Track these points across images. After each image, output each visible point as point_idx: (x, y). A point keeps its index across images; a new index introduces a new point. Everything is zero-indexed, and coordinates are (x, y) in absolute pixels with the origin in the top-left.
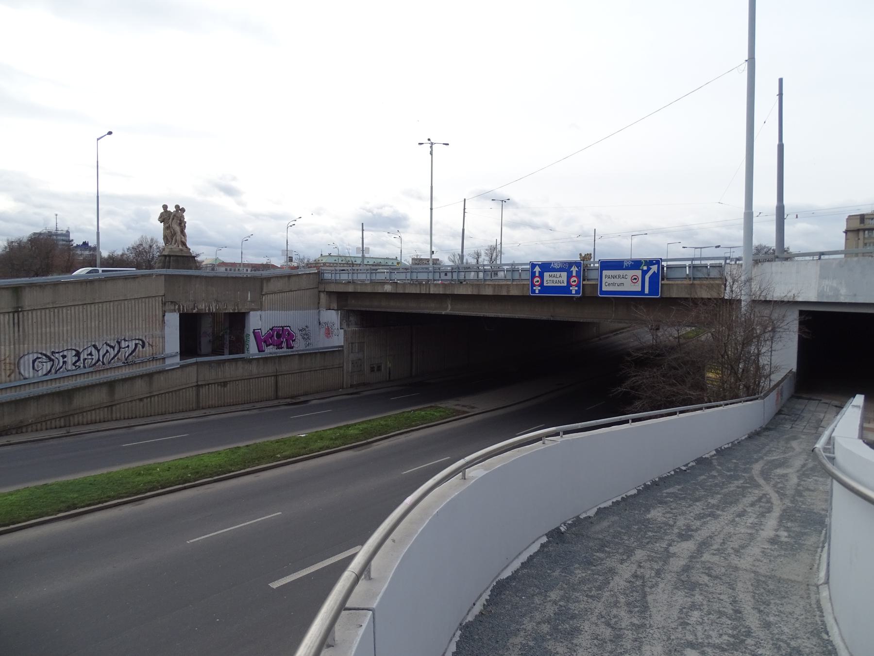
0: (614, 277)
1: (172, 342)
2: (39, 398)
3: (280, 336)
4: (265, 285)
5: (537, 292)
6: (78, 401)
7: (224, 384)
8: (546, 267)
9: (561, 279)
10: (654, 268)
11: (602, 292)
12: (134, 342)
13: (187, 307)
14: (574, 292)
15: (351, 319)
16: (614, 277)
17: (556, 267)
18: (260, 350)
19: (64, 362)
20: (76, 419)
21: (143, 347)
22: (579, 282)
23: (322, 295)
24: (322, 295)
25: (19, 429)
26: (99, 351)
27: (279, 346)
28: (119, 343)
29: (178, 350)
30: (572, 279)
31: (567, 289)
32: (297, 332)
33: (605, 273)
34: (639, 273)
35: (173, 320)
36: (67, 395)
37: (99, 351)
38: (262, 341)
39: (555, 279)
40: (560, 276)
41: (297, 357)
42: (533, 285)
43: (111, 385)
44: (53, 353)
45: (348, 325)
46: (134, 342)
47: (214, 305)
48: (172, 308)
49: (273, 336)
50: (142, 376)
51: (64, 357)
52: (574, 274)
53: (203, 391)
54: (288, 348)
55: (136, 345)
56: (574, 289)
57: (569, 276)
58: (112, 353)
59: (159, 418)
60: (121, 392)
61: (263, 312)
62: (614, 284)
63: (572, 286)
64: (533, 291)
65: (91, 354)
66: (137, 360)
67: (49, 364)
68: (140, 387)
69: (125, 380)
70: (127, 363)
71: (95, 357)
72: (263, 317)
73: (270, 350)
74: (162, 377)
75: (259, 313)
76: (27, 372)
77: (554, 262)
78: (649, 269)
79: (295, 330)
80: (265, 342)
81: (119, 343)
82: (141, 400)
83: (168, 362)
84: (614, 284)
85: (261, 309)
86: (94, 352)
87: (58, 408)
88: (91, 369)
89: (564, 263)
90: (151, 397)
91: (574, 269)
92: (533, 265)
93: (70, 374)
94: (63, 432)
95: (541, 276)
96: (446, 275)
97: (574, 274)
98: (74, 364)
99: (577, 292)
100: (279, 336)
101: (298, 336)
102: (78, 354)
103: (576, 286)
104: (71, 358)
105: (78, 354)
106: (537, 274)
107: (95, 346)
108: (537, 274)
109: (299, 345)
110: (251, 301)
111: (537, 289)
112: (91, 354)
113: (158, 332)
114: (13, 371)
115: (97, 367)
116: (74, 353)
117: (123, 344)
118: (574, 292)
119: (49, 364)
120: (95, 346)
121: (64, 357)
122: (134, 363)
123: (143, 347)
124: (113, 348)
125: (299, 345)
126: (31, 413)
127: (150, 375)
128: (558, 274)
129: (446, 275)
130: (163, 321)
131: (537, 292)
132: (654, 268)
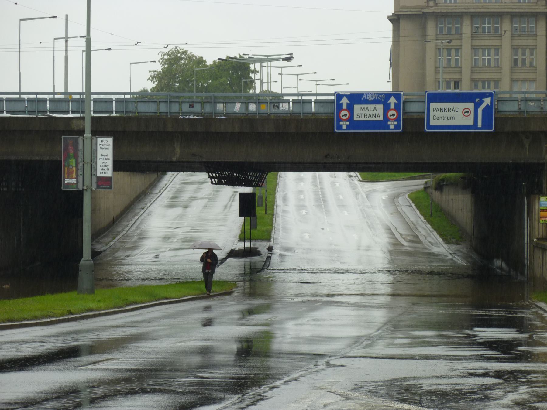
0: (443, 110)
5: (344, 127)
8: (356, 98)
9: (377, 112)
10: (487, 101)
11: (430, 127)
14: (392, 127)
16: (443, 110)
17: (370, 98)
22: (399, 116)
30: (391, 113)
31: (384, 123)
33: (433, 105)
34: (470, 106)
39: (368, 113)
40: (375, 109)
42: (339, 119)
52: (392, 106)
56: (392, 124)
57: (387, 108)
62: (443, 118)
64: (340, 127)
77: (367, 94)
78: (482, 102)
84: (443, 118)
89: (379, 94)
91: (393, 101)
92: (339, 96)
95: (350, 109)
96: (191, 106)
97: (392, 106)
99: (396, 127)
103: (395, 120)
106: (345, 107)
108: (345, 107)
118: (392, 127)
128: (372, 106)
129: (191, 106)
131: (344, 127)
132: (487, 101)
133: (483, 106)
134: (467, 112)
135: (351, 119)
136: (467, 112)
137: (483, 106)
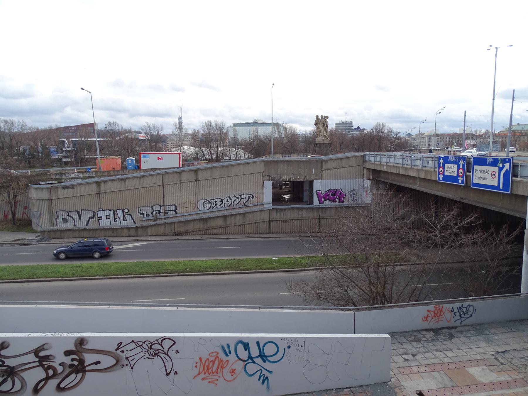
1: (268, 196)
2: (193, 221)
3: (335, 195)
4: (324, 165)
6: (211, 224)
7: (286, 221)
12: (248, 196)
13: (276, 177)
15: (380, 185)
18: (321, 203)
19: (216, 204)
20: (209, 232)
21: (253, 198)
23: (365, 170)
24: (365, 170)
25: (186, 233)
26: (231, 200)
27: (333, 201)
28: (241, 196)
29: (271, 201)
32: (346, 192)
35: (268, 185)
36: (206, 220)
37: (231, 200)
38: (322, 197)
41: (334, 208)
43: (225, 217)
44: (211, 200)
45: (378, 190)
46: (248, 196)
47: (292, 177)
48: (268, 178)
49: (329, 194)
50: (240, 214)
51: (216, 202)
53: (273, 224)
54: (339, 202)
55: (249, 197)
58: (238, 201)
59: (238, 236)
60: (229, 221)
61: (323, 181)
63: (459, 176)
65: (227, 201)
66: (249, 205)
67: (210, 205)
68: (239, 220)
69: (232, 215)
70: (245, 206)
71: (230, 203)
72: (322, 184)
73: (327, 203)
74: (250, 215)
75: (320, 181)
76: (201, 208)
79: (345, 191)
80: (324, 198)
81: (241, 196)
82: (240, 226)
83: (265, 206)
85: (321, 178)
86: (229, 200)
87: (201, 226)
88: (227, 208)
90: (244, 225)
93: (218, 210)
94: (199, 237)
98: (220, 205)
100: (333, 194)
101: (348, 196)
102: (222, 201)
104: (219, 203)
105: (222, 201)
107: (229, 197)
109: (347, 202)
110: (315, 174)
111: (441, 176)
112: (227, 201)
113: (260, 191)
114: (195, 207)
115: (231, 207)
116: (220, 200)
117: (243, 197)
119: (210, 205)
120: (229, 197)
121: (216, 202)
122: (247, 206)
123: (253, 198)
124: (238, 198)
125: (347, 202)
126: (191, 227)
127: (244, 214)
130: (263, 185)
133: (504, 170)
134: (494, 175)
135: (443, 174)
136: (494, 175)
137: (504, 170)
